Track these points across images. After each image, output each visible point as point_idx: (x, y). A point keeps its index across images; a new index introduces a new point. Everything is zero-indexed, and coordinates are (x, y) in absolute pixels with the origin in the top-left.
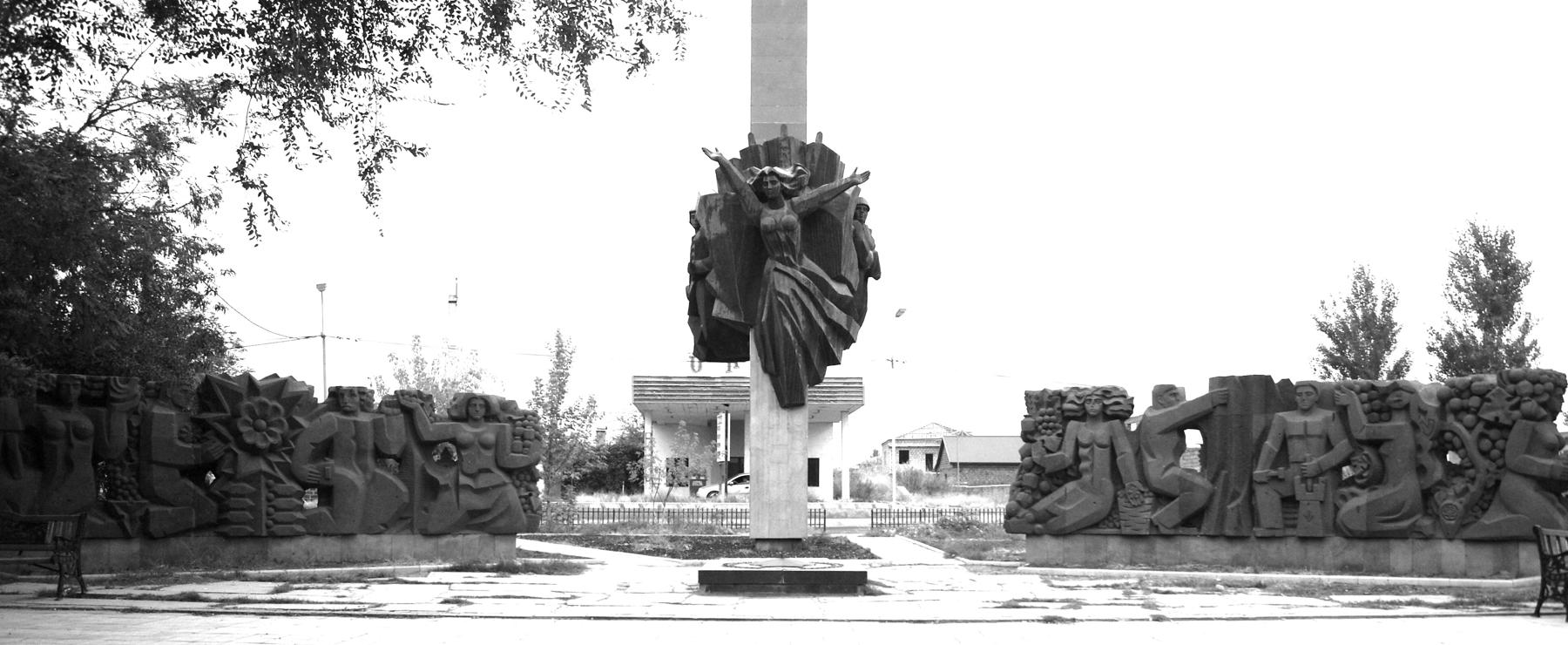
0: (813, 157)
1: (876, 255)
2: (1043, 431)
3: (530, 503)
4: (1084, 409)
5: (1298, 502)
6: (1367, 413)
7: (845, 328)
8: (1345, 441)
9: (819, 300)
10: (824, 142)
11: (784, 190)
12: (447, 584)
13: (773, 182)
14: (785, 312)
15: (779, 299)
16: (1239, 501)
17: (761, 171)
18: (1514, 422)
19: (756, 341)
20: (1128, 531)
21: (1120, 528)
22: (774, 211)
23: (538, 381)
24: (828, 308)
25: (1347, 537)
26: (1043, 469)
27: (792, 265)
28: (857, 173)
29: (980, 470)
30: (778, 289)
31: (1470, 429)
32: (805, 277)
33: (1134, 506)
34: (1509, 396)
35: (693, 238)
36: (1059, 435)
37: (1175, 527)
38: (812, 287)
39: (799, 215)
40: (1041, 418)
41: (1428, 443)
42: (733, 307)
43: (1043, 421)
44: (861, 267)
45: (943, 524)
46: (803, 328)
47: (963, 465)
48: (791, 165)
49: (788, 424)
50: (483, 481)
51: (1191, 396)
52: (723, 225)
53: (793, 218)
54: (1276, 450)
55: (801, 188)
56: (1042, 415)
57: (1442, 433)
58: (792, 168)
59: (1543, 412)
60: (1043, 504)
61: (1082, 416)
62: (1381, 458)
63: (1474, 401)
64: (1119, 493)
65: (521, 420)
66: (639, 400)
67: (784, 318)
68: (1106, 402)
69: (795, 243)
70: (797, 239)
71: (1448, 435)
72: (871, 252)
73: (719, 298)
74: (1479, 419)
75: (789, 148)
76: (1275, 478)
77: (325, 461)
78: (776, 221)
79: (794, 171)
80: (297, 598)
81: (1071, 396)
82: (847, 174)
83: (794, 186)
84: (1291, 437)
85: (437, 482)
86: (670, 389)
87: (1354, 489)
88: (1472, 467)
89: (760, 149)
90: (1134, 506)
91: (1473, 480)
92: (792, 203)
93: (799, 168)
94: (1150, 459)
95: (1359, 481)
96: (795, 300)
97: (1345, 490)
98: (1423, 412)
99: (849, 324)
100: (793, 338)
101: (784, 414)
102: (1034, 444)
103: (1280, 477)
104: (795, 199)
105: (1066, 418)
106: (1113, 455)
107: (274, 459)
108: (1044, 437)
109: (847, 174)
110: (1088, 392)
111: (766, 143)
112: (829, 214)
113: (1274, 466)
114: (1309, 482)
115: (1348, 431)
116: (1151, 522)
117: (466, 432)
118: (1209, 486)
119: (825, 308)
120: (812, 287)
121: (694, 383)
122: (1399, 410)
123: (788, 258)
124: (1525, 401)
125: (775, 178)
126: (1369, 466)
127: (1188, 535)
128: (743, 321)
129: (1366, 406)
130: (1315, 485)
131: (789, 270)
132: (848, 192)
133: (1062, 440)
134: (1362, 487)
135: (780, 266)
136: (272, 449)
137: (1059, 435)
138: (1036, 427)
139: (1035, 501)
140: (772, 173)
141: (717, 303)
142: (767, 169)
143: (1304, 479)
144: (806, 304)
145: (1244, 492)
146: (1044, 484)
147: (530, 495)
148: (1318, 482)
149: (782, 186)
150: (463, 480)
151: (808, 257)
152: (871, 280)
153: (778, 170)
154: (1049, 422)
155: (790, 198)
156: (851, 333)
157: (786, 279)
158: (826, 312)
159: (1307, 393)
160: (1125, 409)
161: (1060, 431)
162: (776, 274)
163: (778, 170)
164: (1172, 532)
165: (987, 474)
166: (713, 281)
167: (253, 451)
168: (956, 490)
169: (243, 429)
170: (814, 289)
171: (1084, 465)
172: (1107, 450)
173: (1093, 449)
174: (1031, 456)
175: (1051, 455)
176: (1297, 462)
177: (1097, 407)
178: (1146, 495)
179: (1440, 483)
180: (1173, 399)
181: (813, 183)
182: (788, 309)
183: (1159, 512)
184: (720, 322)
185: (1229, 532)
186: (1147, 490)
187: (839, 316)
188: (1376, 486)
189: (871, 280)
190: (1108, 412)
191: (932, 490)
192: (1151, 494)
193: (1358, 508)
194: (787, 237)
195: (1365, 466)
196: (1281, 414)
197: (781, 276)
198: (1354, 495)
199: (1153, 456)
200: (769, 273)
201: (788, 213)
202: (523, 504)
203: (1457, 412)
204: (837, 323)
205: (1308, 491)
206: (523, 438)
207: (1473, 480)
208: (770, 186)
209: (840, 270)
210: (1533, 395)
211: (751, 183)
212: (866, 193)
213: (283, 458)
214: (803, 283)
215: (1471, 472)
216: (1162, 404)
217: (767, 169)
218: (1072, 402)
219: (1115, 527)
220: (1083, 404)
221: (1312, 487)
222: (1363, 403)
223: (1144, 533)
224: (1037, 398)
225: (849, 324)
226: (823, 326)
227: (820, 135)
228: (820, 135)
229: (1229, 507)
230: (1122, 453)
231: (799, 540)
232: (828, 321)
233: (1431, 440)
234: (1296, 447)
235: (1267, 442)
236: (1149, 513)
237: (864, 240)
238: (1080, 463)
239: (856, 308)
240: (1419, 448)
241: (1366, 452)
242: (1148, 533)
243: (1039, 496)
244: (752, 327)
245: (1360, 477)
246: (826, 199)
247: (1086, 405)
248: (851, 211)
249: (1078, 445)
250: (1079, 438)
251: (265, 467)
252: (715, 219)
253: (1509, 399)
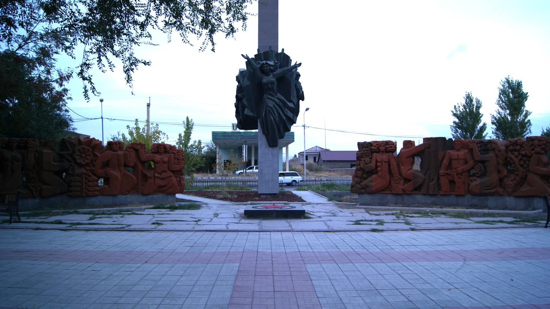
0: (281, 58)
1: (303, 92)
2: (364, 157)
3: (181, 183)
4: (379, 149)
5: (455, 182)
6: (480, 151)
7: (292, 118)
8: (472, 161)
9: (283, 109)
10: (284, 52)
11: (271, 70)
12: (152, 214)
13: (267, 67)
14: (271, 113)
15: (269, 108)
16: (434, 182)
17: (262, 62)
18: (532, 155)
19: (260, 123)
20: (394, 192)
21: (392, 191)
22: (267, 77)
23: (180, 135)
24: (286, 112)
25: (472, 195)
26: (365, 170)
27: (273, 96)
28: (297, 63)
29: (333, 163)
30: (268, 105)
31: (516, 157)
32: (278, 100)
33: (397, 184)
34: (530, 145)
35: (237, 86)
36: (370, 158)
37: (411, 191)
38: (281, 104)
40: (363, 152)
41: (501, 162)
42: (252, 111)
43: (364, 153)
44: (298, 96)
45: (324, 185)
46: (277, 119)
47: (328, 161)
48: (273, 60)
49: (272, 153)
50: (164, 175)
51: (417, 144)
52: (249, 82)
53: (274, 79)
54: (447, 164)
55: (277, 69)
56: (364, 151)
57: (506, 158)
58: (273, 61)
59: (543, 151)
60: (364, 183)
61: (378, 151)
62: (485, 167)
63: (518, 147)
64: (391, 179)
65: (178, 153)
66: (215, 140)
67: (271, 115)
68: (387, 146)
69: (274, 88)
70: (275, 87)
71: (509, 159)
72: (301, 91)
73: (247, 108)
74: (520, 154)
75: (272, 54)
76: (447, 174)
77: (106, 168)
78: (268, 81)
79: (274, 63)
80: (100, 222)
81: (374, 144)
82: (293, 64)
83: (274, 68)
84: (453, 159)
85: (147, 175)
86: (226, 136)
87: (475, 178)
88: (517, 170)
89: (262, 55)
90: (397, 184)
91: (518, 175)
92: (273, 74)
93: (276, 62)
94: (402, 167)
95: (477, 175)
97: (472, 178)
98: (500, 151)
99: (293, 117)
101: (271, 149)
102: (361, 161)
103: (449, 173)
104: (274, 73)
105: (373, 152)
106: (389, 165)
107: (88, 168)
108: (365, 159)
109: (293, 64)
110: (380, 143)
111: (264, 52)
113: (447, 170)
114: (459, 175)
115: (473, 158)
116: (403, 189)
117: (158, 157)
118: (423, 176)
119: (285, 112)
120: (281, 104)
121: (234, 134)
122: (491, 150)
123: (272, 94)
124: (536, 148)
125: (267, 65)
126: (480, 170)
127: (416, 194)
128: (256, 116)
129: (479, 148)
130: (461, 176)
131: (272, 98)
132: (293, 70)
133: (371, 160)
134: (478, 177)
135: (269, 97)
136: (87, 164)
137: (370, 158)
138: (362, 155)
139: (361, 182)
140: (267, 63)
141: (246, 109)
142: (264, 62)
143: (457, 174)
144: (278, 110)
145: (436, 178)
146: (365, 176)
147: (181, 180)
148: (462, 175)
150: (156, 175)
151: (279, 93)
152: (301, 101)
153: (269, 62)
154: (367, 153)
155: (273, 72)
156: (294, 120)
157: (272, 102)
158: (286, 113)
159: (458, 144)
160: (393, 149)
161: (370, 157)
162: (268, 99)
163: (269, 62)
164: (410, 193)
165: (335, 164)
166: (245, 101)
167: (80, 165)
168: (325, 171)
169: (76, 157)
171: (379, 169)
172: (387, 163)
173: (382, 163)
174: (360, 165)
175: (367, 165)
176: (455, 168)
177: (384, 148)
178: (401, 179)
179: (506, 176)
180: (410, 145)
181: (281, 67)
182: (272, 112)
183: (405, 186)
184: (247, 116)
185: (431, 193)
186: (401, 178)
187: (290, 114)
188: (483, 177)
189: (301, 101)
190: (388, 150)
191: (317, 170)
192: (403, 179)
193: (477, 185)
194: (272, 87)
195: (479, 170)
196: (449, 151)
197: (270, 100)
198: (475, 180)
199: (404, 166)
200: (265, 99)
201: (272, 78)
202: (178, 183)
203: (511, 151)
205: (459, 179)
206: (178, 160)
207: (518, 175)
208: (266, 68)
209: (290, 98)
210: (539, 145)
211: (259, 67)
212: (299, 70)
213: (91, 168)
214: (278, 103)
215: (517, 172)
216: (407, 147)
217: (264, 62)
218: (375, 146)
219: (390, 191)
220: (379, 147)
221: (460, 177)
222: (478, 147)
223: (400, 193)
224: (362, 145)
225: (293, 117)
226: (284, 118)
227: (283, 50)
228: (283, 50)
229: (431, 184)
230: (392, 165)
231: (276, 194)
232: (286, 116)
233: (503, 161)
234: (454, 163)
235: (444, 161)
236: (402, 186)
237: (299, 87)
238: (377, 168)
239: (296, 111)
240: (498, 164)
241: (479, 165)
242: (402, 193)
243: (363, 180)
244: (259, 118)
245: (477, 173)
246: (285, 73)
247: (380, 147)
248: (294, 77)
249: (377, 162)
250: (377, 159)
251: (84, 171)
252: (246, 79)
253: (530, 147)
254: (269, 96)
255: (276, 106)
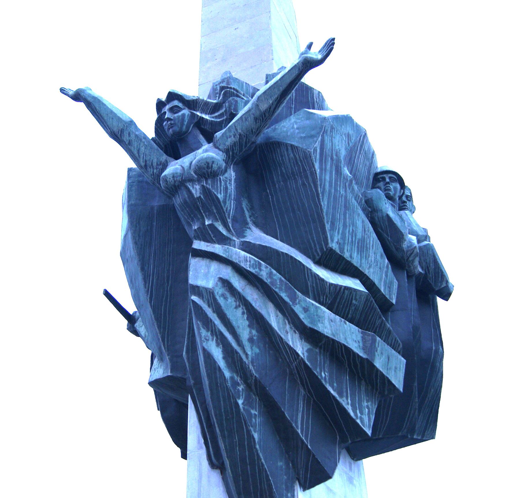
9: (284, 295)
11: (200, 123)
14: (207, 323)
24: (306, 310)
27: (223, 240)
32: (248, 255)
39: (227, 151)
69: (220, 196)
96: (231, 300)
100: (227, 374)
112: (287, 145)
119: (298, 309)
131: (217, 249)
149: (193, 115)
157: (214, 266)
158: (302, 316)
170: (270, 274)
194: (205, 191)
204: (333, 340)
209: (327, 243)
214: (247, 266)
254: (203, 243)
255: (238, 283)
